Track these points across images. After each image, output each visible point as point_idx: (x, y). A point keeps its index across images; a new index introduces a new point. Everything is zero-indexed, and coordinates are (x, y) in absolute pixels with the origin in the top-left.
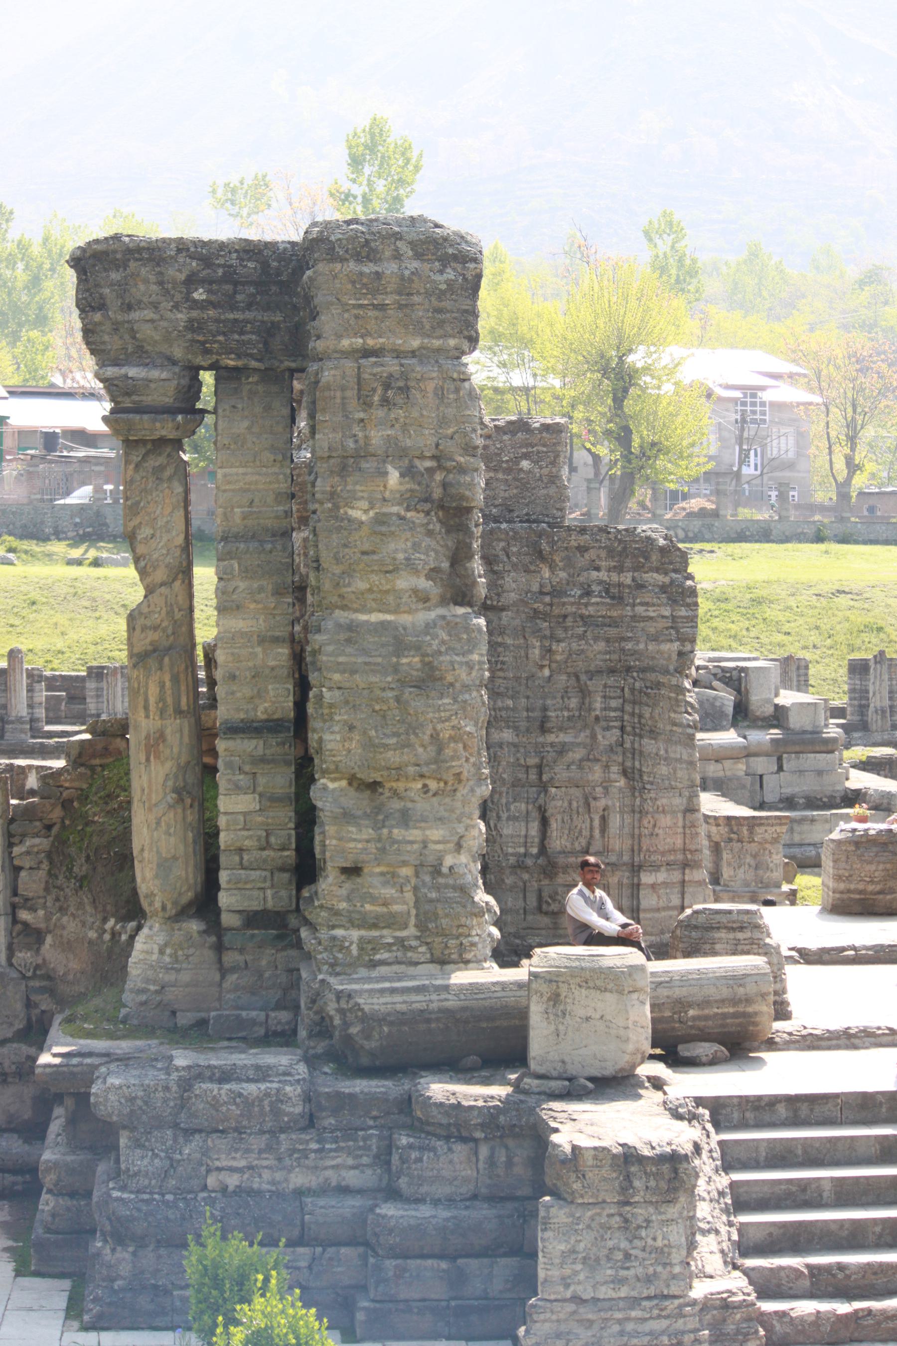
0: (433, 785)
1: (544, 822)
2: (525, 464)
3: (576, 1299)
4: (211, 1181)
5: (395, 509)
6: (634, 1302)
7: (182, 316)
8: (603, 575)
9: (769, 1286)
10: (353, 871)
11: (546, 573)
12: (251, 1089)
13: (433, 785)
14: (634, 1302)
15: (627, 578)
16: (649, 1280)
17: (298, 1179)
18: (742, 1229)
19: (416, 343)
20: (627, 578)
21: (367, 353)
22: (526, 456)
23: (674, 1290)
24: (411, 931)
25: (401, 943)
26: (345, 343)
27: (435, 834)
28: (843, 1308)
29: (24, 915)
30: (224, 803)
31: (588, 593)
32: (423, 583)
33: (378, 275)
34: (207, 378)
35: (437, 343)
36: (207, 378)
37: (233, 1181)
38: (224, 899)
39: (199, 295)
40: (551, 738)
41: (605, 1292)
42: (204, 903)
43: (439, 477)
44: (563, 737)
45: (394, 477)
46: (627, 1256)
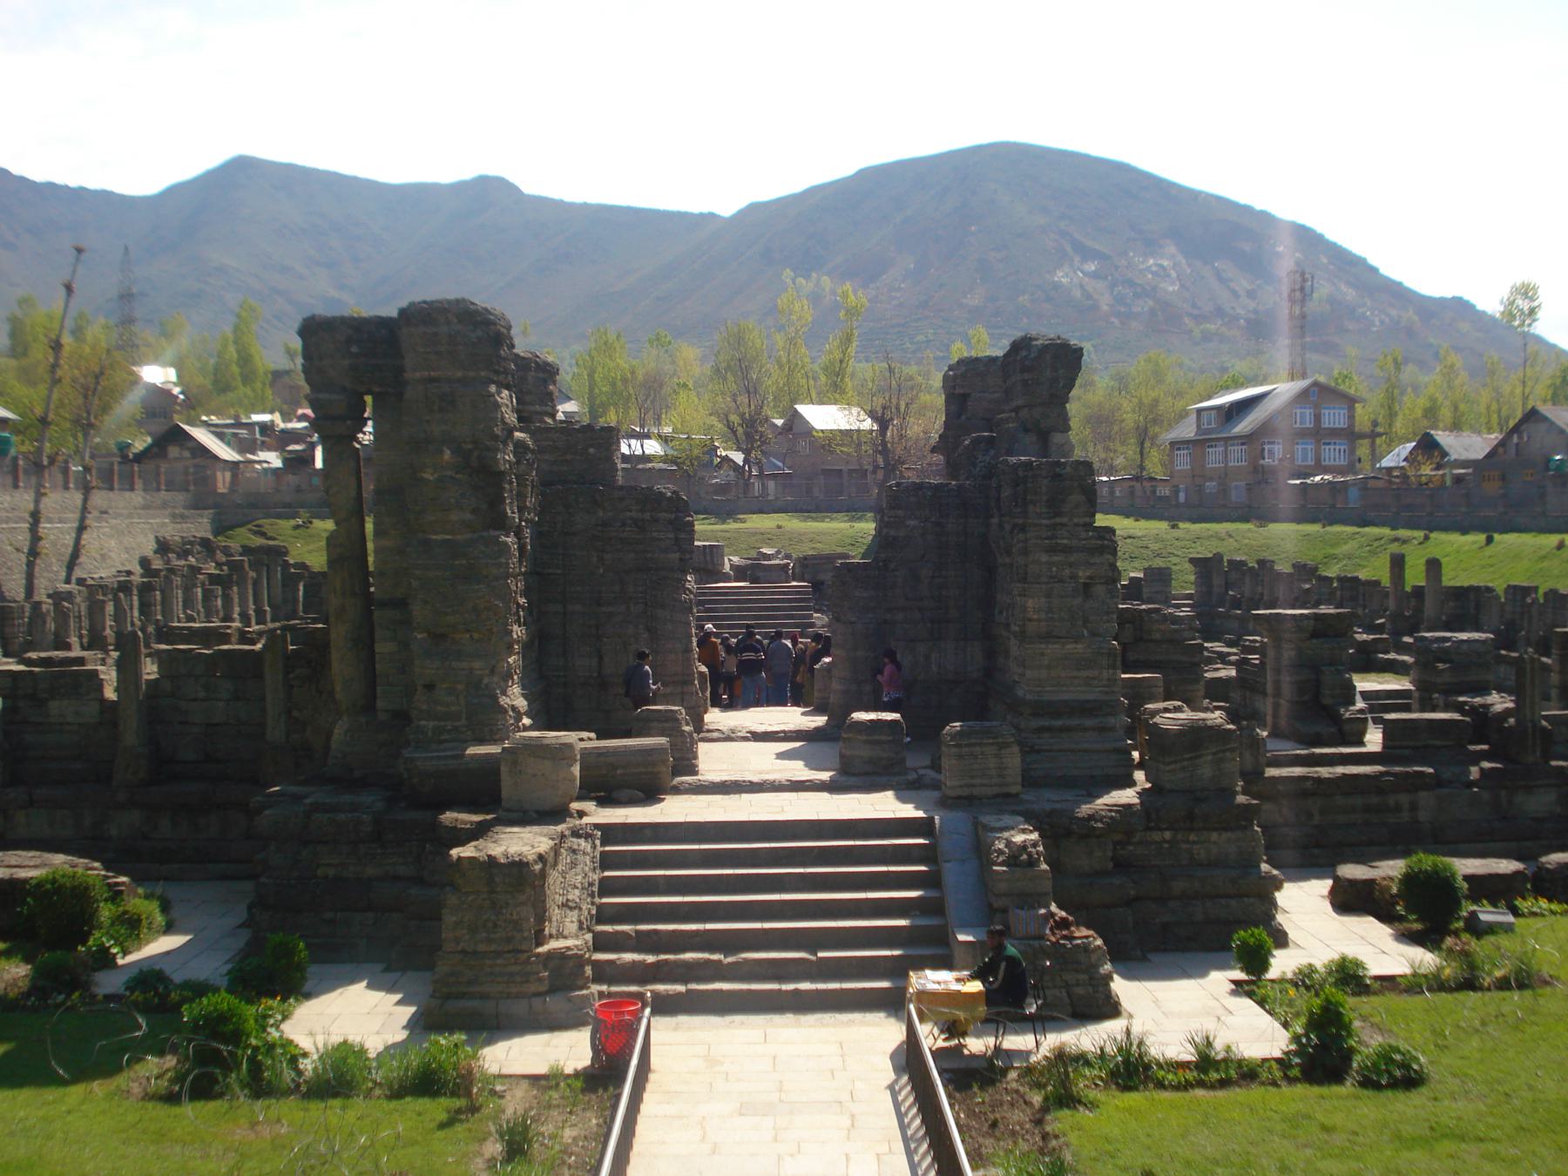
0: (476, 636)
1: (601, 658)
2: (592, 450)
3: (464, 952)
4: (320, 872)
5: (449, 473)
6: (498, 954)
7: (346, 362)
8: (633, 514)
9: (601, 943)
10: (430, 687)
11: (601, 514)
12: (342, 817)
13: (476, 636)
14: (498, 954)
15: (647, 516)
16: (509, 940)
17: (370, 871)
18: (600, 907)
19: (459, 374)
20: (647, 516)
21: (432, 380)
22: (592, 446)
23: (524, 947)
24: (463, 722)
25: (456, 729)
26: (418, 375)
27: (477, 665)
28: (650, 959)
29: (295, 713)
30: (379, 648)
31: (624, 524)
32: (468, 516)
33: (436, 334)
34: (369, 399)
35: (472, 374)
36: (369, 399)
37: (331, 872)
38: (380, 704)
39: (354, 349)
40: (603, 609)
41: (482, 947)
42: (369, 706)
43: (476, 454)
44: (610, 609)
45: (447, 454)
46: (495, 926)
